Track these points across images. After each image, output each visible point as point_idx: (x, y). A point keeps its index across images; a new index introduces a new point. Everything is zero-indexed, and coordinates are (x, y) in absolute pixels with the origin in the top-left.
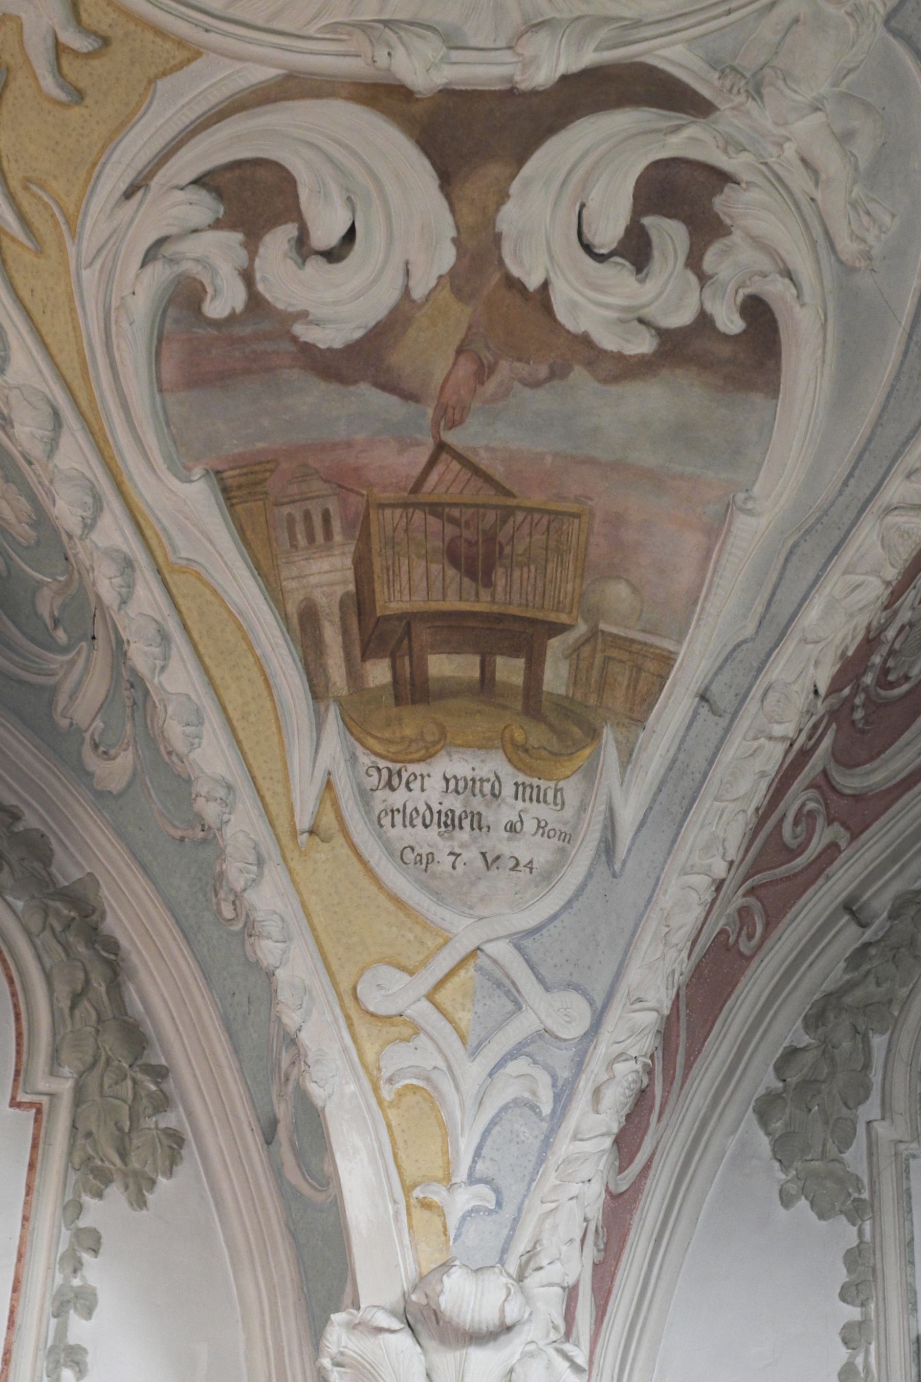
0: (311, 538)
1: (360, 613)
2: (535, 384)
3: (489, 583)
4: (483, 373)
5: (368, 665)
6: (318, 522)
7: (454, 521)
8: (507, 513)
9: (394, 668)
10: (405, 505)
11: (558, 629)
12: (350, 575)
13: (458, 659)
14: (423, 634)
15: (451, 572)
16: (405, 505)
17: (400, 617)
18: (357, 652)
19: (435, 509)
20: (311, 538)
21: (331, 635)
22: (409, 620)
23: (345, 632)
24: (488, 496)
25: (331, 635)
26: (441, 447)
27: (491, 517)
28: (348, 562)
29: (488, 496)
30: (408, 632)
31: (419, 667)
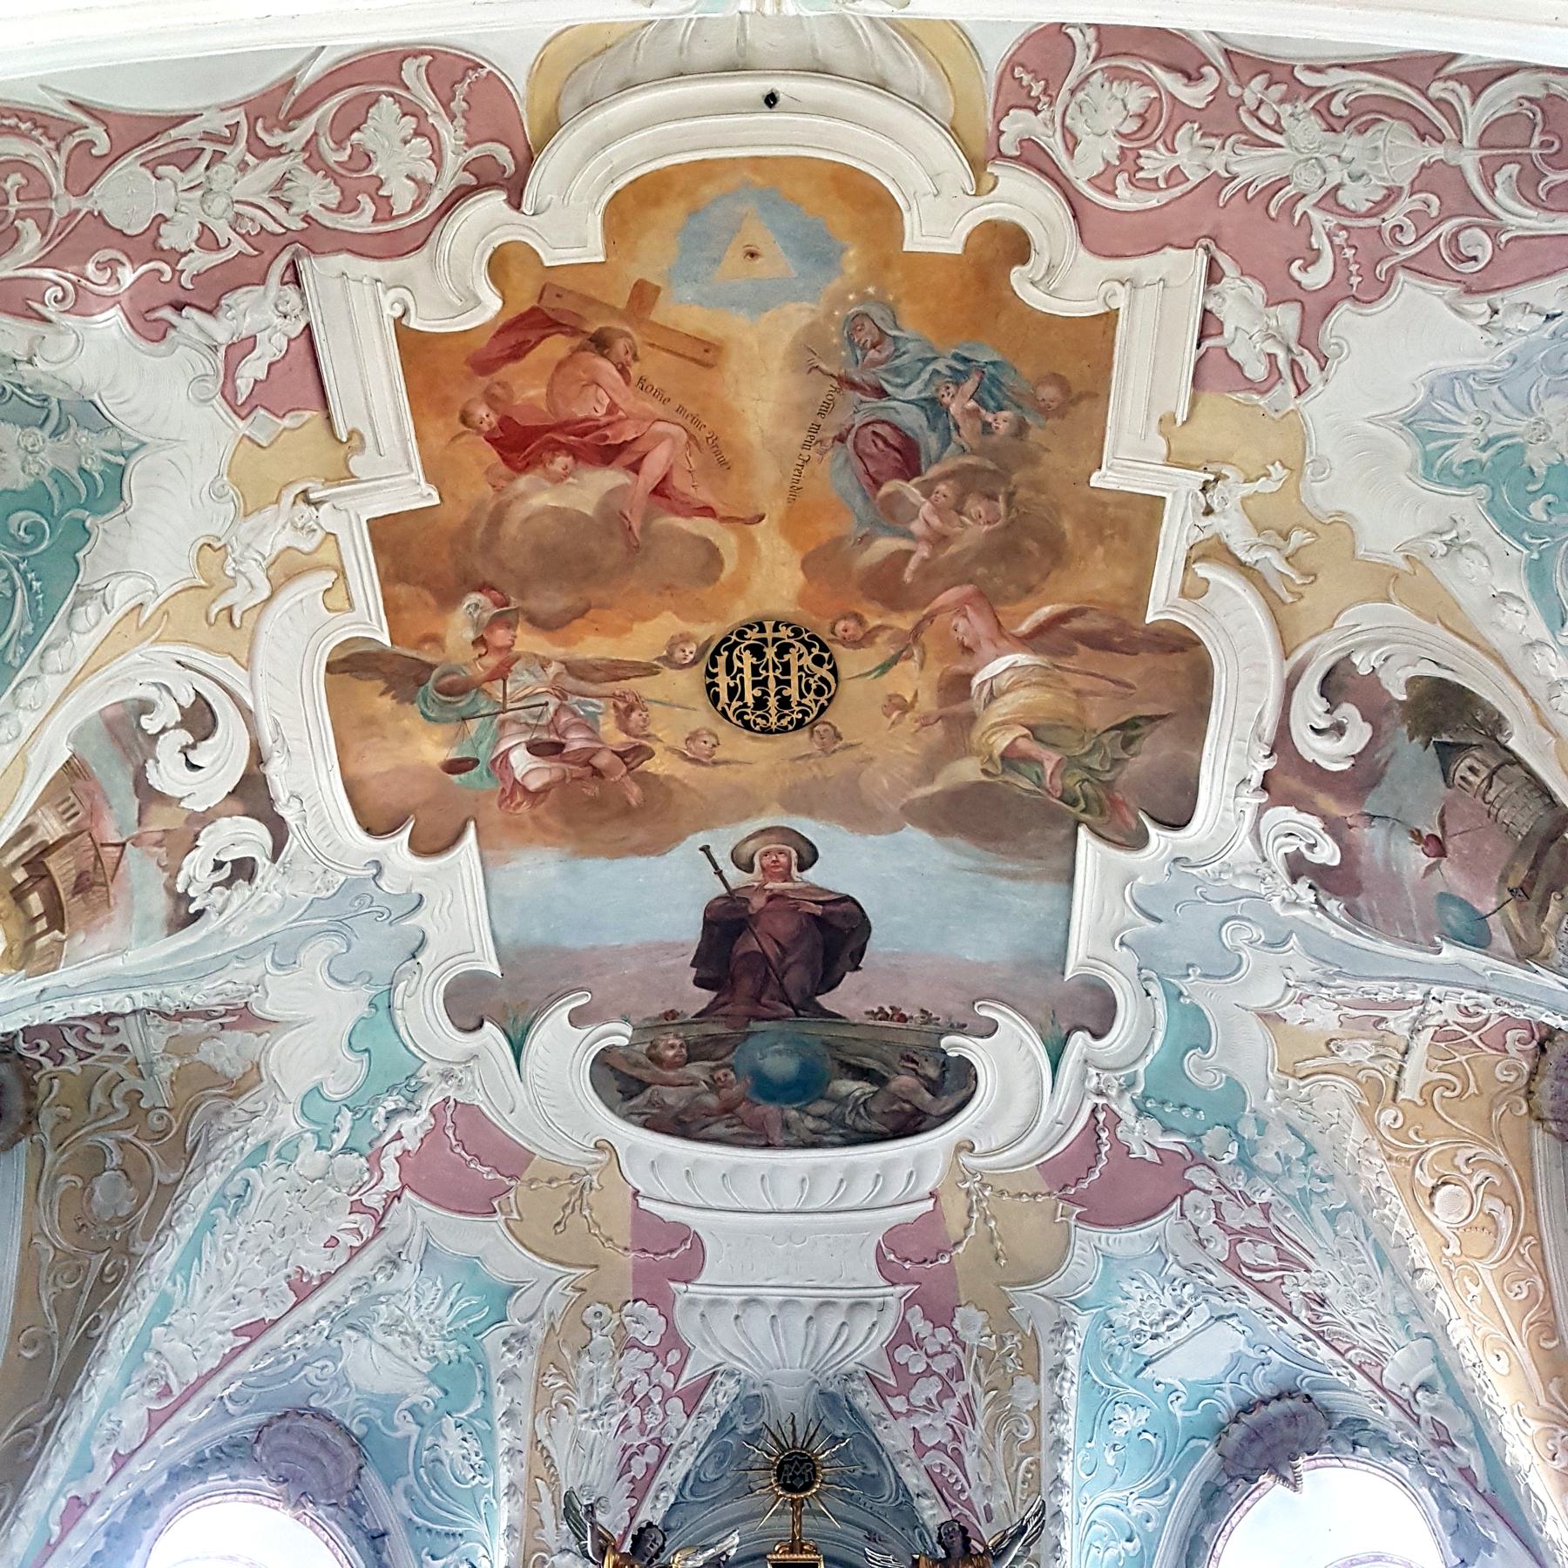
0: (64, 812)
1: (41, 853)
2: (159, 864)
3: (73, 896)
4: (159, 844)
5: (22, 869)
6: (72, 811)
7: (95, 867)
8: (105, 884)
9: (25, 881)
10: (94, 844)
11: (62, 931)
12: (56, 838)
13: (40, 903)
14: (43, 885)
15: (74, 879)
16: (94, 844)
17: (48, 871)
18: (24, 861)
19: (98, 857)
20: (64, 812)
21: (26, 845)
22: (47, 875)
23: (31, 850)
24: (109, 872)
25: (26, 845)
26: (124, 845)
27: (102, 880)
28: (61, 834)
29: (109, 872)
30: (43, 877)
31: (30, 891)
